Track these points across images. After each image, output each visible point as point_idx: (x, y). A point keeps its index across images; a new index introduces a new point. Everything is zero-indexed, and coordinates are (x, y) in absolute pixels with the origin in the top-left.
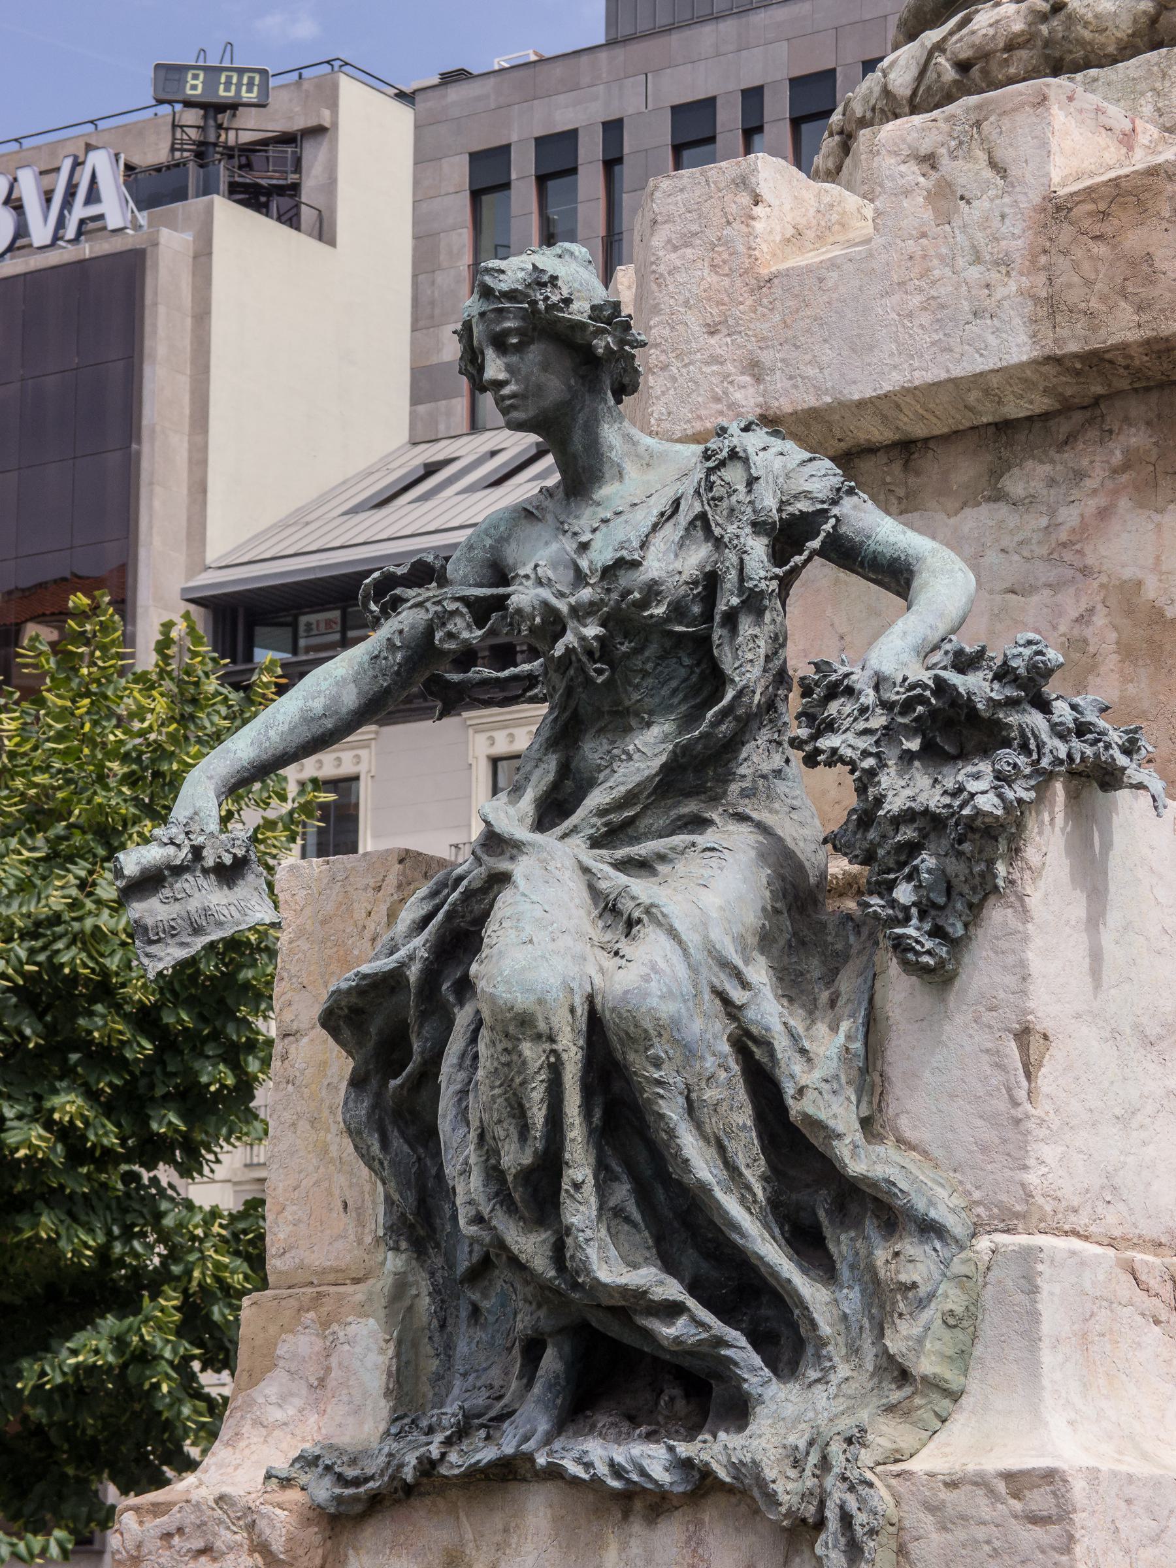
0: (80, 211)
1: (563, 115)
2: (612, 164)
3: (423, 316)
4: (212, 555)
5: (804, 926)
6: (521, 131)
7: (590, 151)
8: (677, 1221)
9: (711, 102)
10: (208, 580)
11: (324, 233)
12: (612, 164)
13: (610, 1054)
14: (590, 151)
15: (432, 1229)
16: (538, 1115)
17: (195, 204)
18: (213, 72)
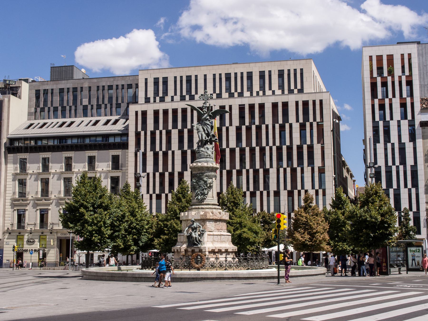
1: (47, 87)
2: (52, 93)
3: (29, 107)
4: (9, 133)
5: (199, 235)
6: (42, 88)
7: (50, 92)
8: (196, 241)
9: (63, 89)
10: (9, 136)
11: (20, 97)
12: (52, 93)
13: (196, 238)
14: (50, 92)
17: (8, 95)
18: (9, 81)
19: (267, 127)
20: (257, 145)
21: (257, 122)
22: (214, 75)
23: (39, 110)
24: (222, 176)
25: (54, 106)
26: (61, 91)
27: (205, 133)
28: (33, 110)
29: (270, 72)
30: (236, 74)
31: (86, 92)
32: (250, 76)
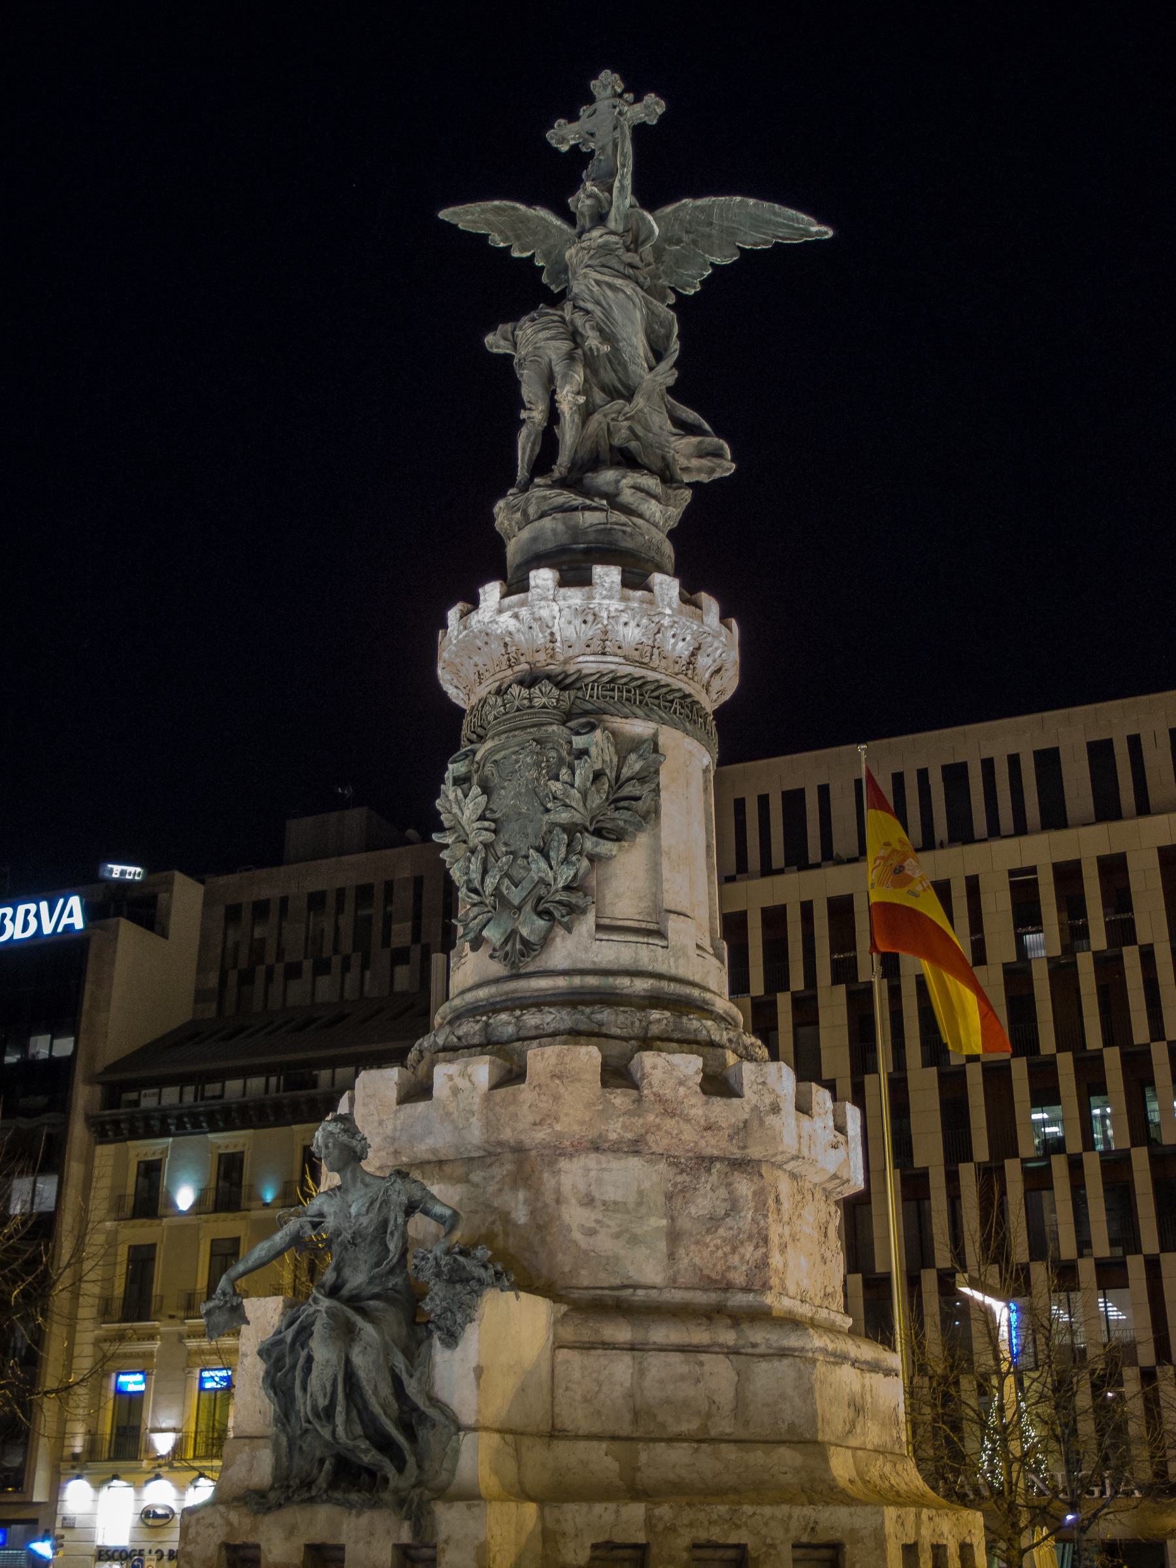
0: (65, 920)
3: (201, 969)
11: (164, 934)
15: (288, 1421)
16: (329, 1389)
19: (1147, 955)
20: (1108, 1042)
21: (1098, 940)
22: (898, 780)
23: (233, 977)
24: (959, 1197)
25: (287, 959)
26: (316, 901)
27: (590, 362)
28: (213, 980)
29: (1134, 742)
30: (988, 766)
31: (404, 898)
32: (1048, 761)
